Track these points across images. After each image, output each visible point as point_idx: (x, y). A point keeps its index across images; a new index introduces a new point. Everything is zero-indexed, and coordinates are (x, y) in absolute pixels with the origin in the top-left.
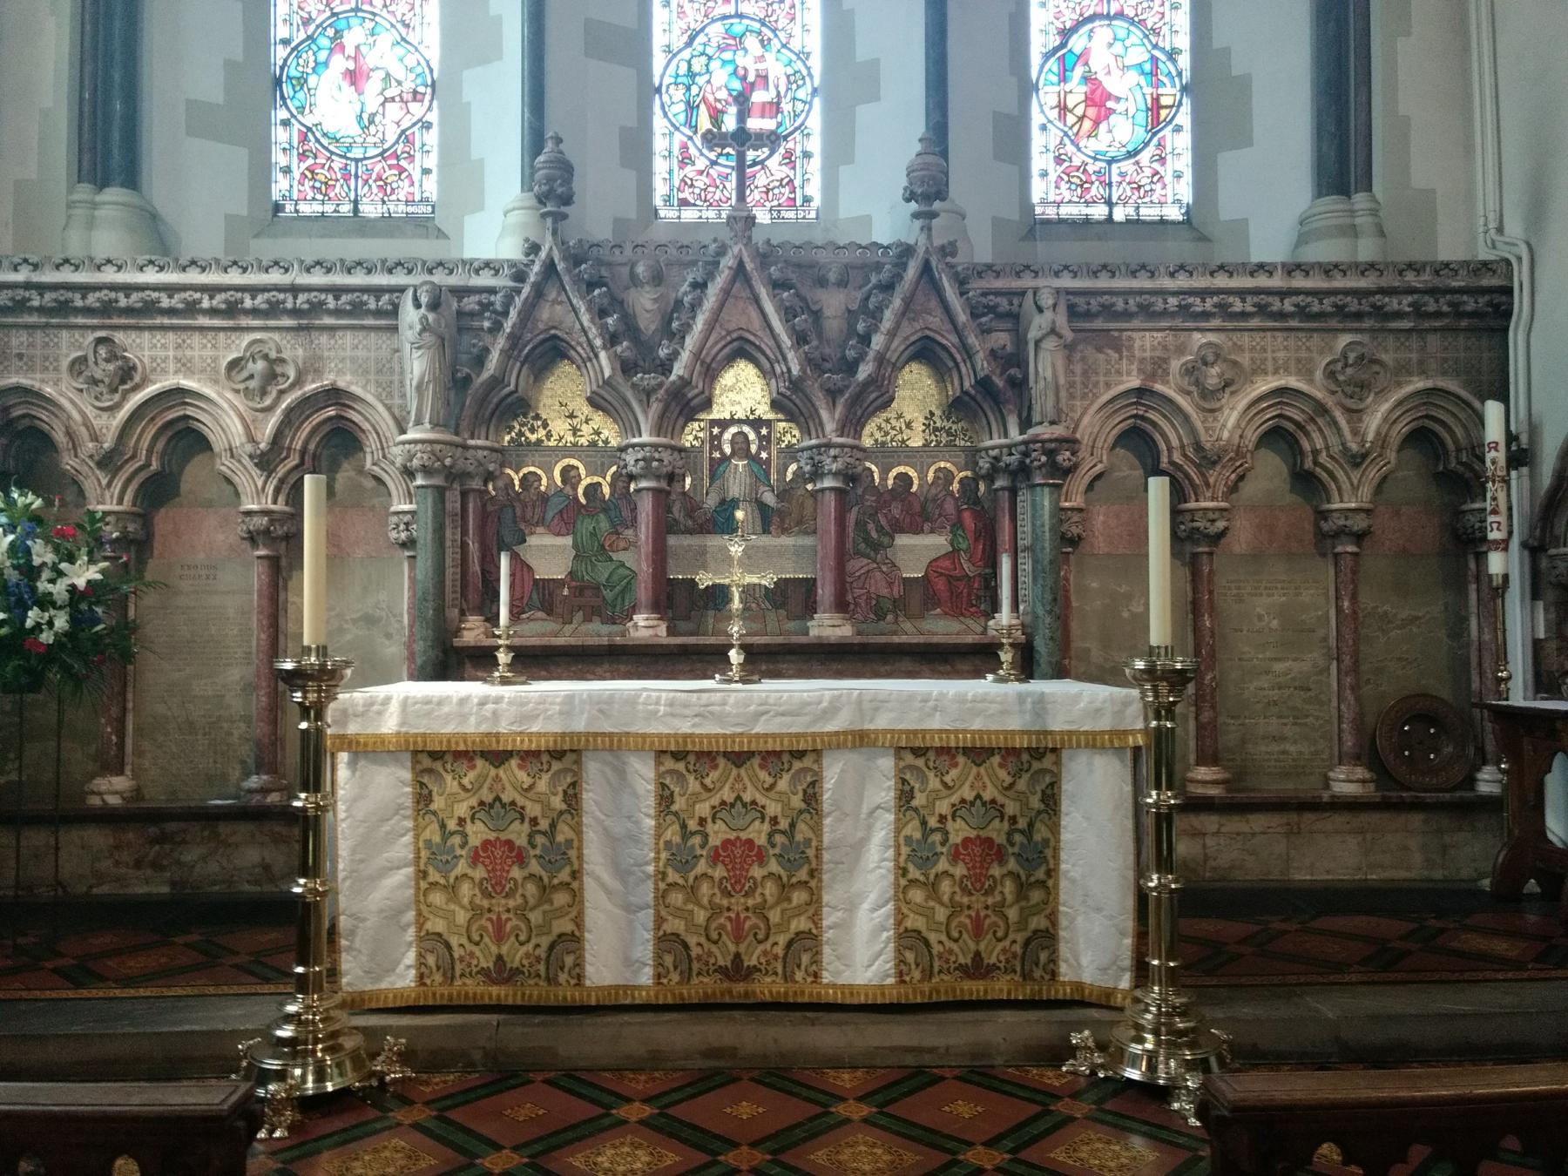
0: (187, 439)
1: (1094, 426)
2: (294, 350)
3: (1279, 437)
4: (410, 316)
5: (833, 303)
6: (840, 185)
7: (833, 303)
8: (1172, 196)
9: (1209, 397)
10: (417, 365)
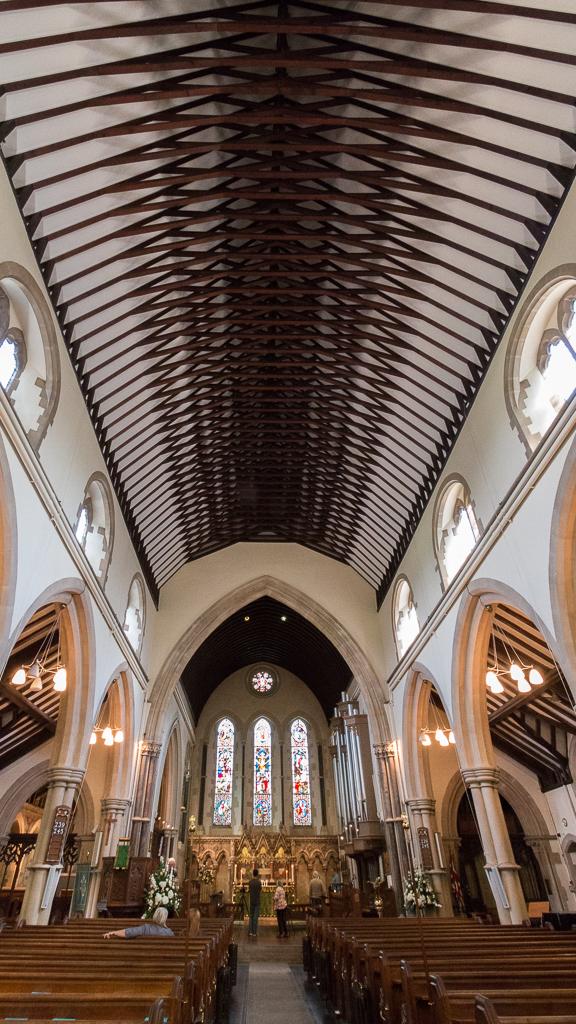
0: (209, 857)
1: (298, 856)
2: (219, 846)
3: (317, 857)
4: (232, 843)
5: (272, 840)
6: (272, 821)
7: (272, 840)
8: (309, 823)
9: (310, 852)
10: (232, 849)
